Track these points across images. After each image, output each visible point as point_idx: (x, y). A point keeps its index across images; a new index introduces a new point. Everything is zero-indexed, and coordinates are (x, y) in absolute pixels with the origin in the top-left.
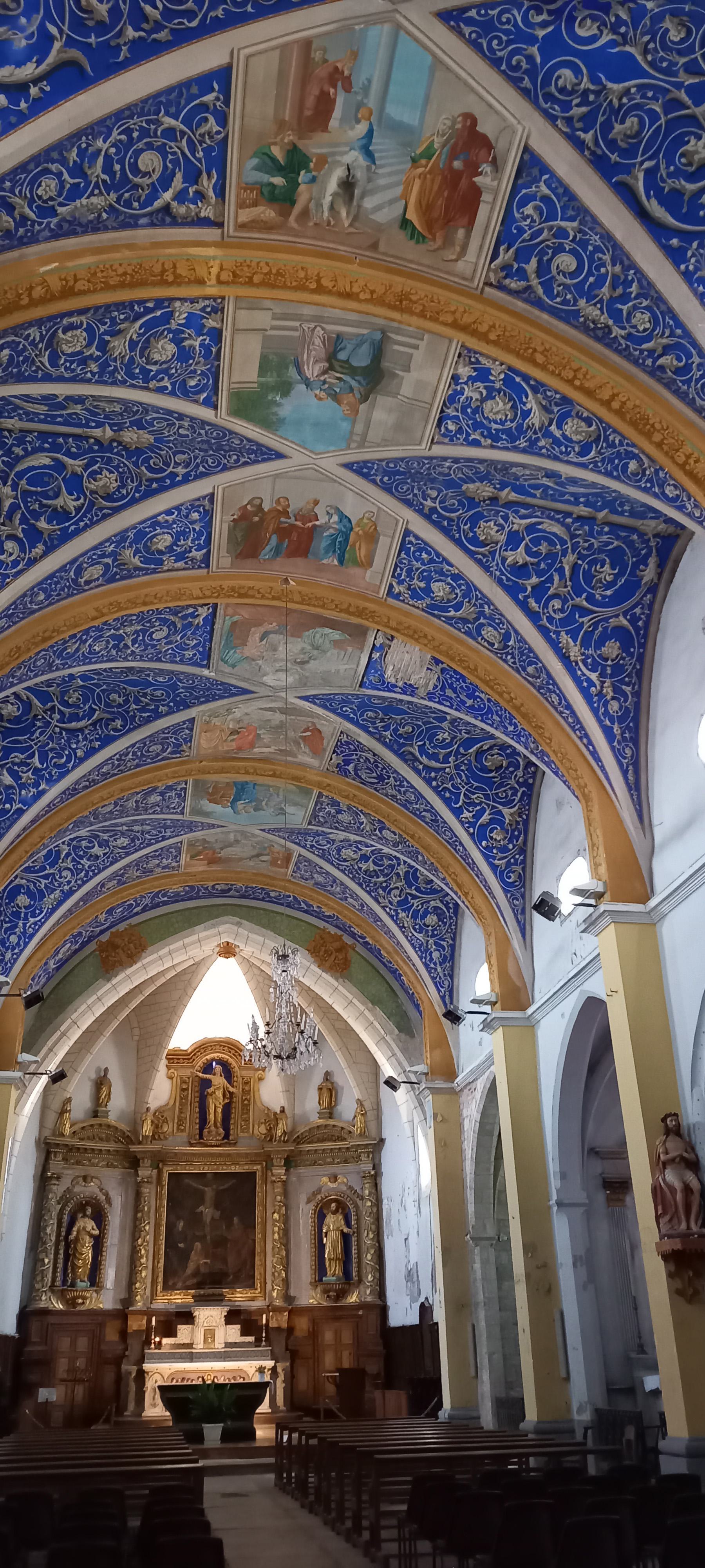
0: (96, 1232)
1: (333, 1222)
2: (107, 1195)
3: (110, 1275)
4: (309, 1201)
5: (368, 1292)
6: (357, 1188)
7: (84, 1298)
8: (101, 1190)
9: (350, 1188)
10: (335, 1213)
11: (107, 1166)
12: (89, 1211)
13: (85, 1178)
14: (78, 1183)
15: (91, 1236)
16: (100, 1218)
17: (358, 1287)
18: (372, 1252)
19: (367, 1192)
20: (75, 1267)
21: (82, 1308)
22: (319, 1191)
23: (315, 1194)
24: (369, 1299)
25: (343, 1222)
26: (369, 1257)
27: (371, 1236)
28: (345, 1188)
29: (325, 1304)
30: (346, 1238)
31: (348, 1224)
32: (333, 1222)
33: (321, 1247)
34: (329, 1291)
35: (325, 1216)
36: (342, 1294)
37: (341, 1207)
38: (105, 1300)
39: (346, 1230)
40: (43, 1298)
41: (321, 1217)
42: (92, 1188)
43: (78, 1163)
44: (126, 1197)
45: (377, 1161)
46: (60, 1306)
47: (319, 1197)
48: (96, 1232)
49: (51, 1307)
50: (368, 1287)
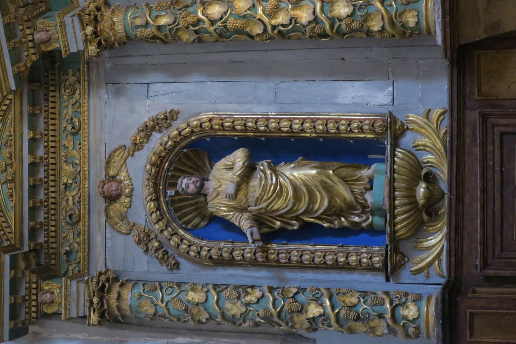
0: (239, 157)
2: (147, 131)
3: (353, 100)
7: (418, 172)
8: (137, 146)
11: (76, 133)
12: (187, 184)
13: (111, 199)
14: (124, 217)
15: (250, 170)
16: (200, 149)
20: (334, 212)
21: (443, 173)
38: (420, 105)
40: (410, 311)
42: (136, 172)
43: (74, 221)
44: (155, 68)
46: (436, 240)
48: (239, 157)
49: (439, 274)
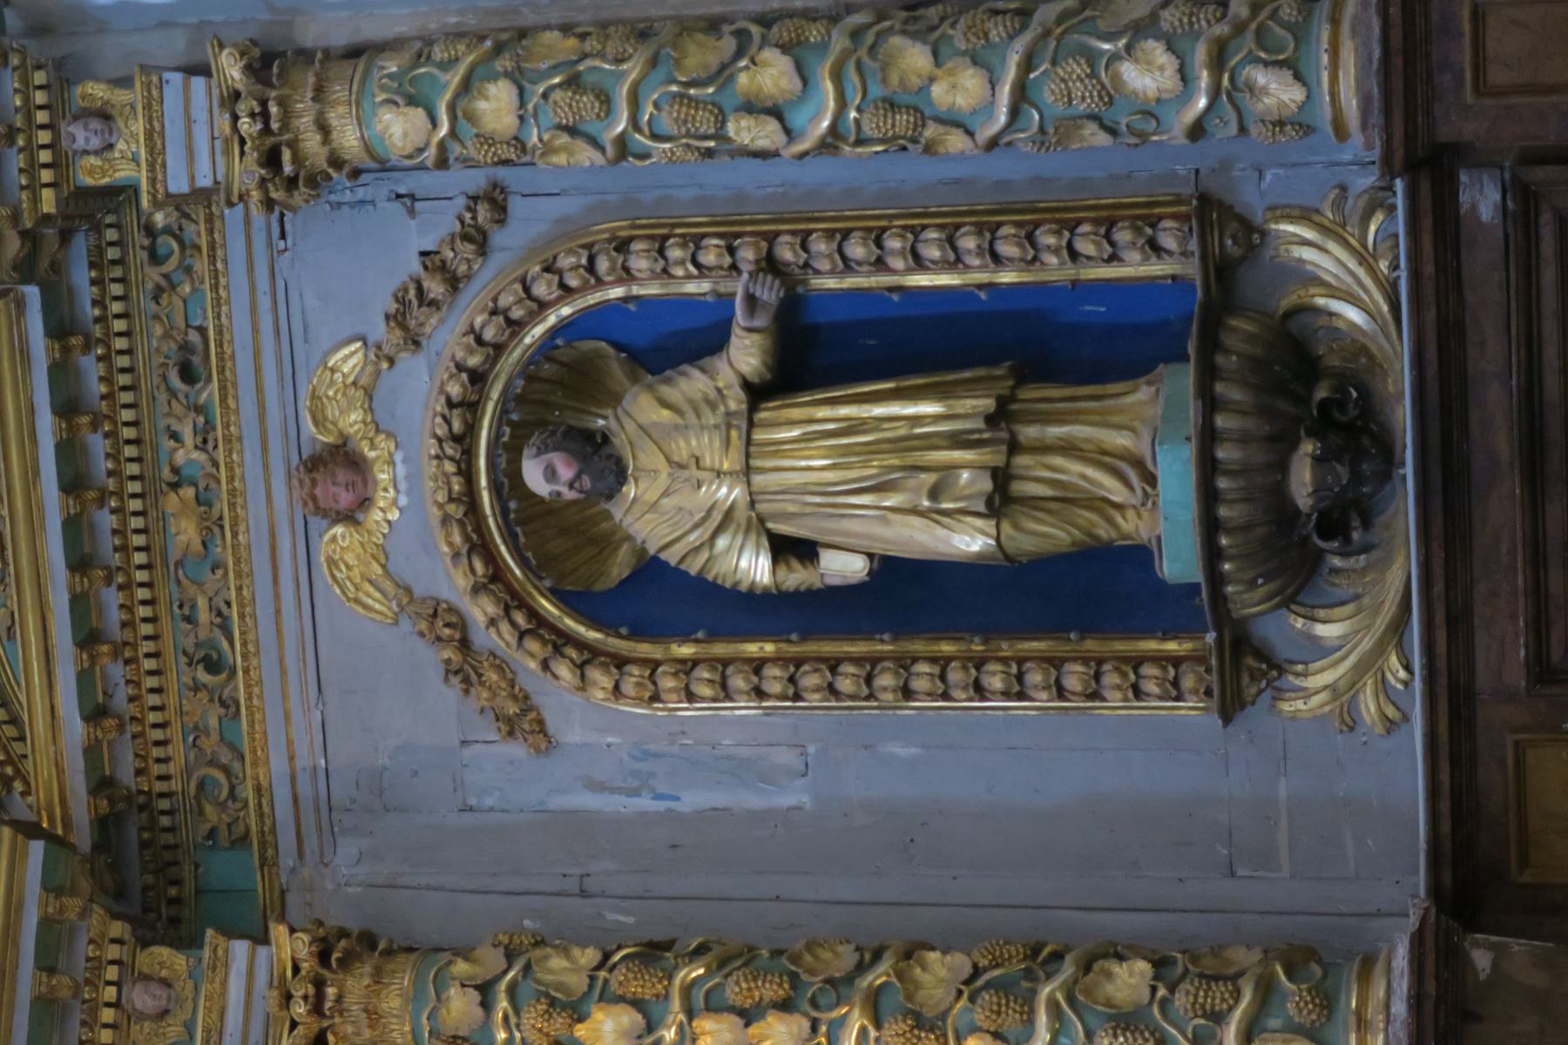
1: (698, 482)
4: (523, 722)
5: (1277, 91)
6: (402, 244)
9: (407, 317)
10: (603, 462)
17: (1252, 235)
18: (915, 58)
19: (399, 128)
22: (444, 624)
23: (466, 663)
24: (1344, 76)
25: (693, 383)
26: (960, 89)
27: (771, 74)
28: (422, 387)
29: (1400, 569)
30: (814, 353)
31: (689, 340)
32: (698, 482)
33: (905, 595)
34: (1282, 512)
35: (652, 570)
36: (1300, 382)
37: (564, 393)
39: (746, 354)
41: (663, 604)
45: (175, 46)
47: (479, 611)
50: (1230, 93)
